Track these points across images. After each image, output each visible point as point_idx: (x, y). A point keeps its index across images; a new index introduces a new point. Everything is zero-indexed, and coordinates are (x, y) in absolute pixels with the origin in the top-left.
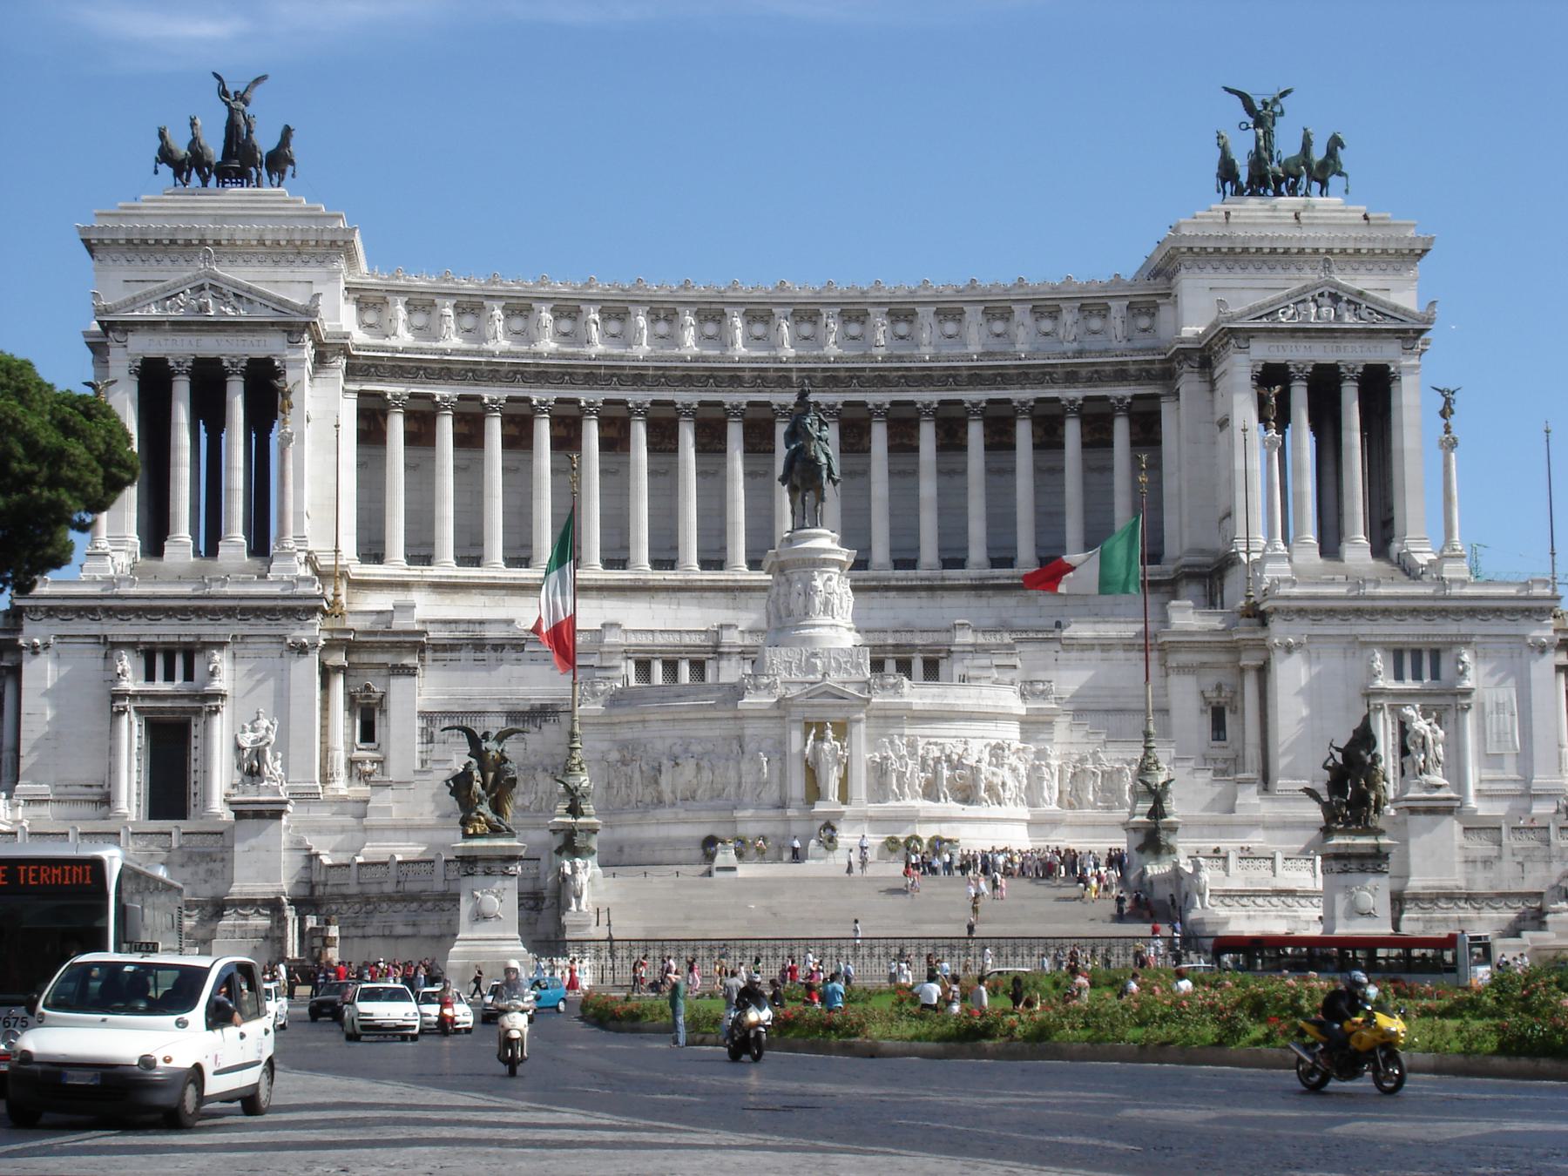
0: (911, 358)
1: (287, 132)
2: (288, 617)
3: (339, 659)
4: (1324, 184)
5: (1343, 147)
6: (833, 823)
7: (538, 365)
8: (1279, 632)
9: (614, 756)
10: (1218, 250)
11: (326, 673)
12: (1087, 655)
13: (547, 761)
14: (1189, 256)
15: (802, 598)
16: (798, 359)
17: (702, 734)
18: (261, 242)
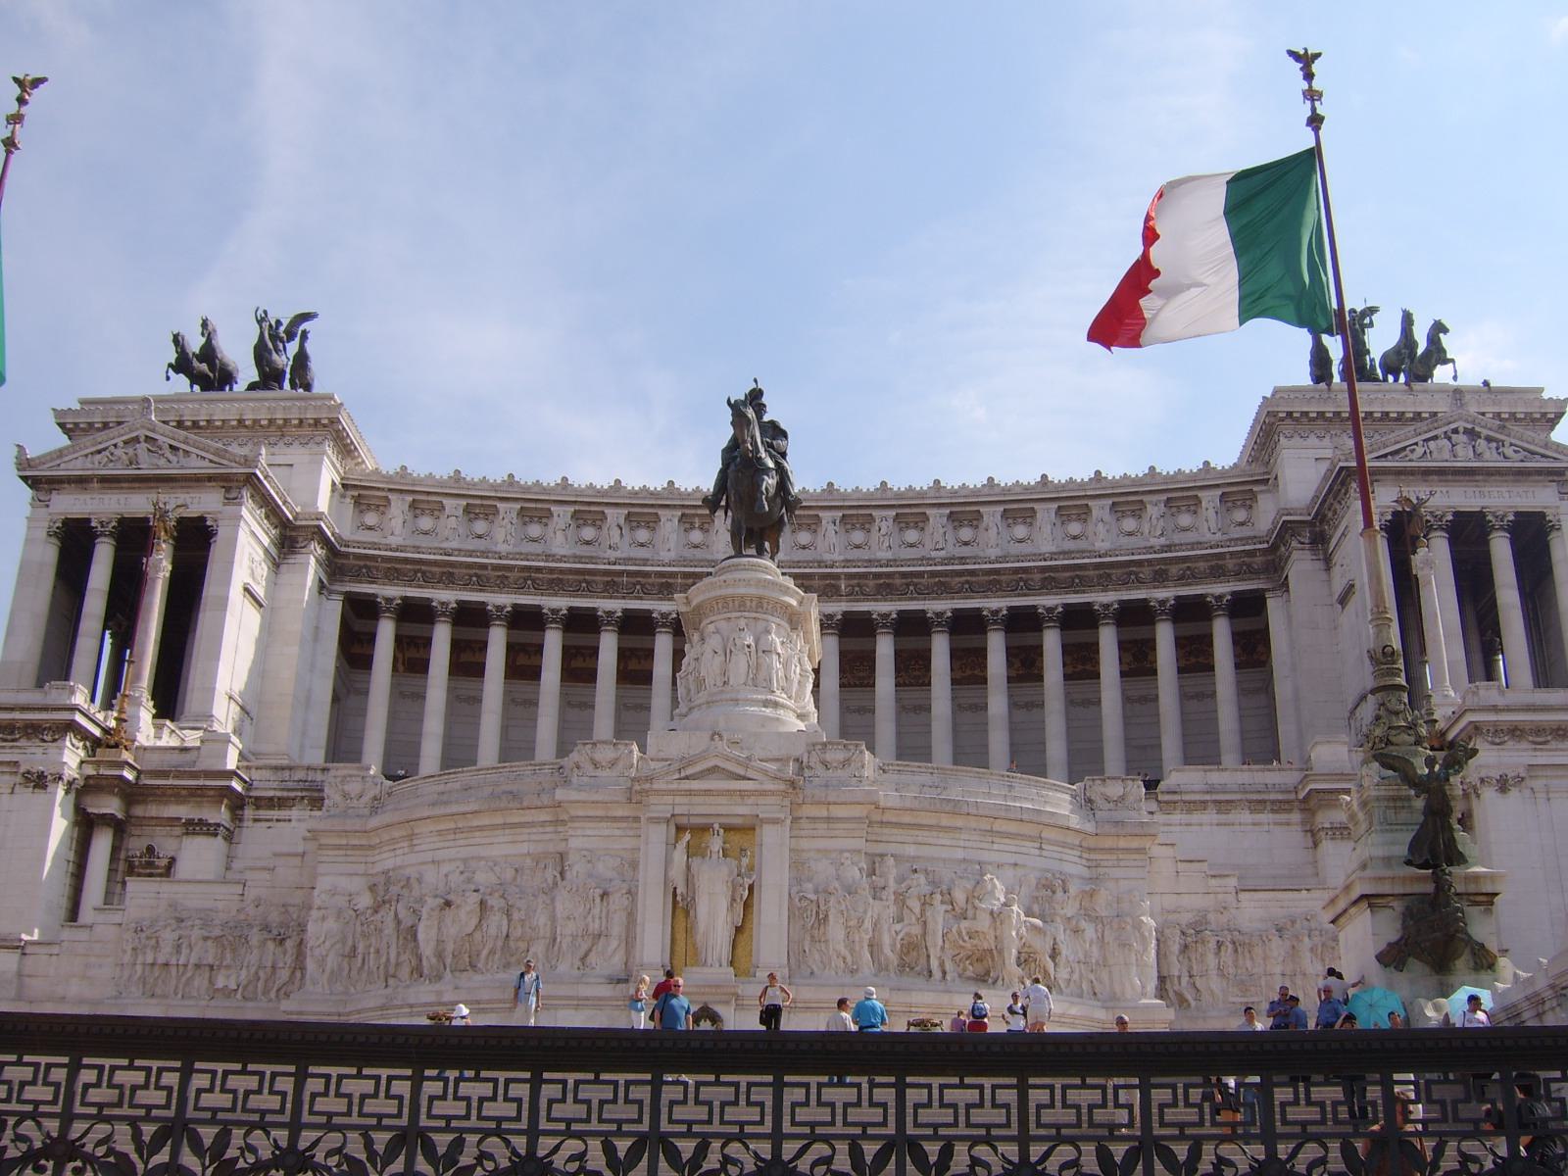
0: (975, 559)
1: (305, 335)
2: (28, 736)
3: (111, 806)
4: (1425, 376)
5: (1445, 330)
6: (719, 1009)
7: (552, 570)
8: (1488, 758)
9: (365, 901)
10: (1321, 414)
11: (85, 825)
12: (1196, 817)
13: (275, 917)
14: (1287, 428)
15: (720, 659)
16: (847, 562)
17: (495, 852)
18: (241, 422)
